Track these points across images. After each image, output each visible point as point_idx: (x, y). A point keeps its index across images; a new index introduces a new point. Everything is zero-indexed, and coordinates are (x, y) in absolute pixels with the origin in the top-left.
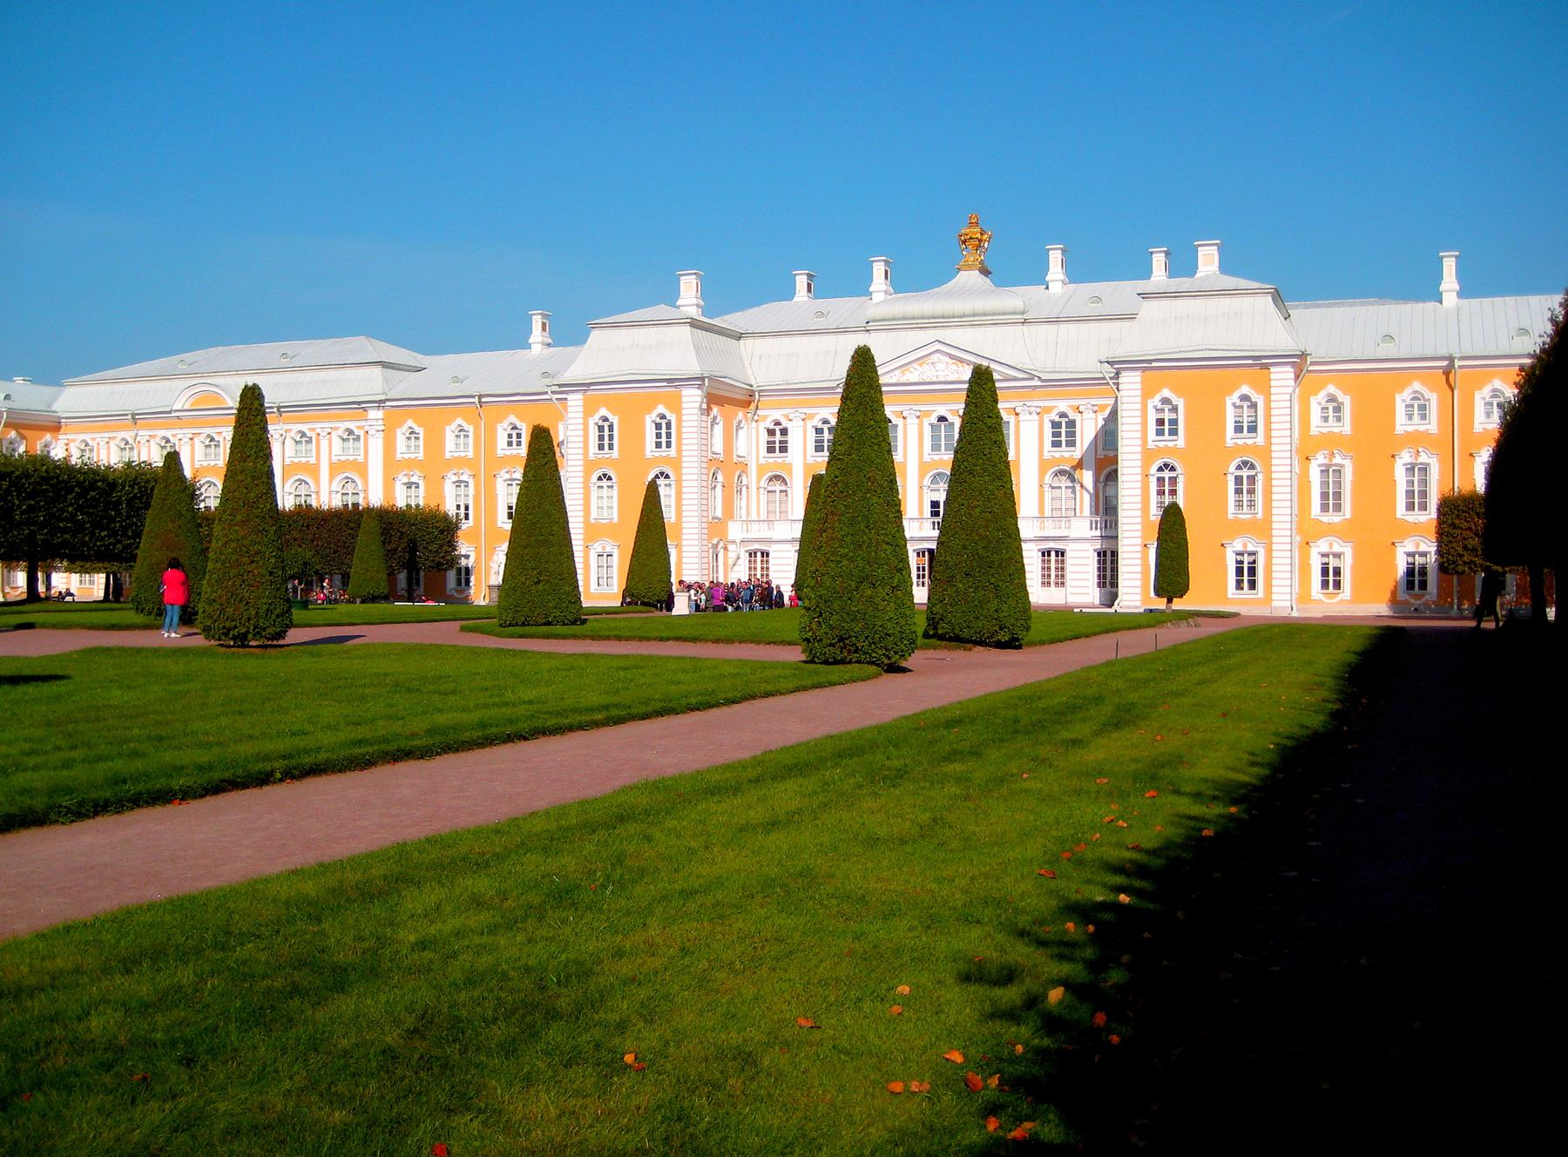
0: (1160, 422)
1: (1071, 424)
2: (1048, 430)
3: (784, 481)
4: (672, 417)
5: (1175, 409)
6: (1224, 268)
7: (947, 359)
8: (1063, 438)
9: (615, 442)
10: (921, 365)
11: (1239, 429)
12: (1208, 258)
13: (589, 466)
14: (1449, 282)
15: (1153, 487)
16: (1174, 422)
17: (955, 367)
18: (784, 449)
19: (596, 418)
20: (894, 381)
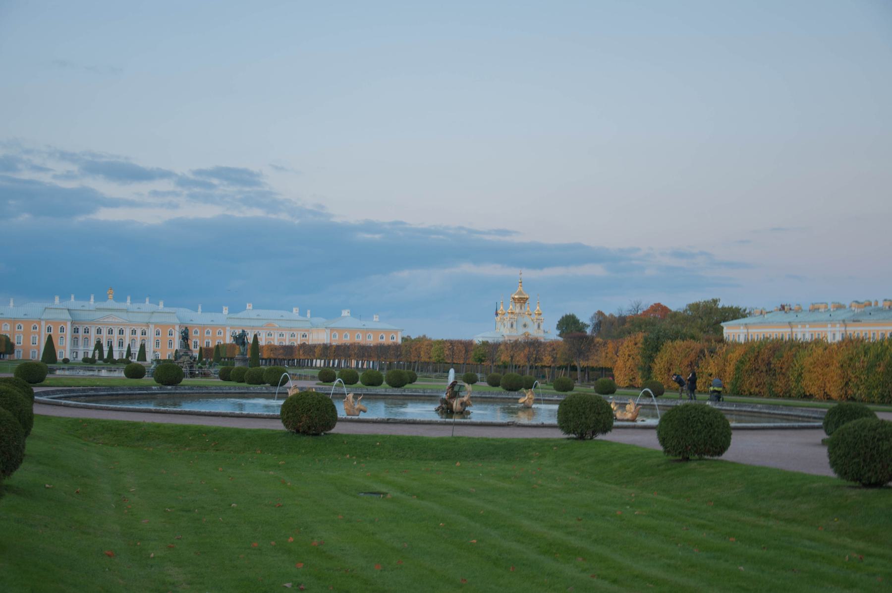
1: (135, 331)
3: (77, 338)
4: (64, 327)
6: (165, 306)
9: (52, 330)
11: (170, 335)
12: (161, 306)
13: (45, 334)
14: (200, 310)
18: (78, 332)
19: (47, 326)
20: (101, 321)
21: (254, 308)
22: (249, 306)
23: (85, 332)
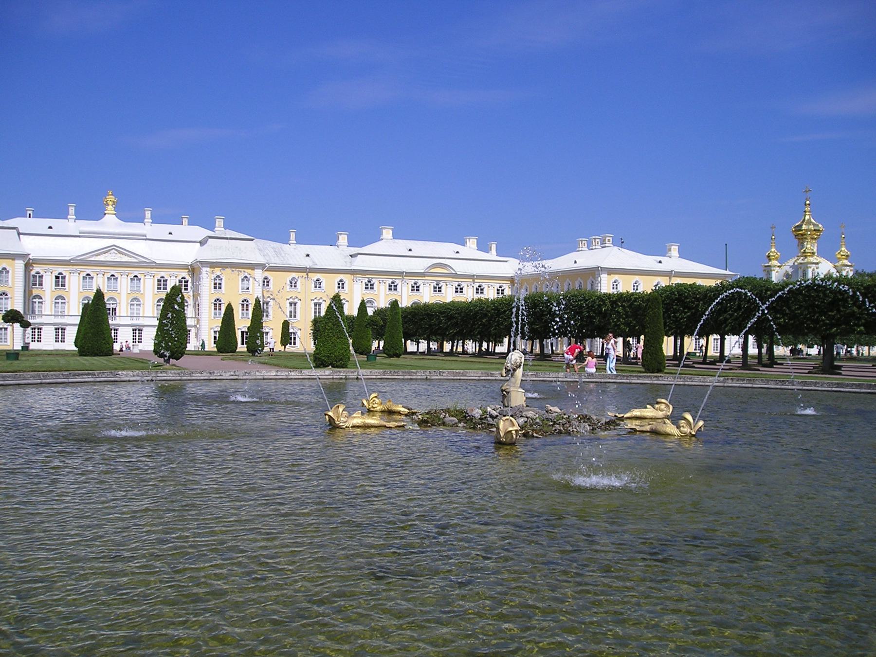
0: (215, 284)
2: (156, 283)
5: (221, 279)
7: (116, 252)
8: (162, 286)
10: (105, 253)
12: (219, 222)
15: (213, 307)
16: (220, 284)
17: (119, 255)
20: (93, 259)
21: (395, 237)
22: (387, 233)
23: (57, 284)
